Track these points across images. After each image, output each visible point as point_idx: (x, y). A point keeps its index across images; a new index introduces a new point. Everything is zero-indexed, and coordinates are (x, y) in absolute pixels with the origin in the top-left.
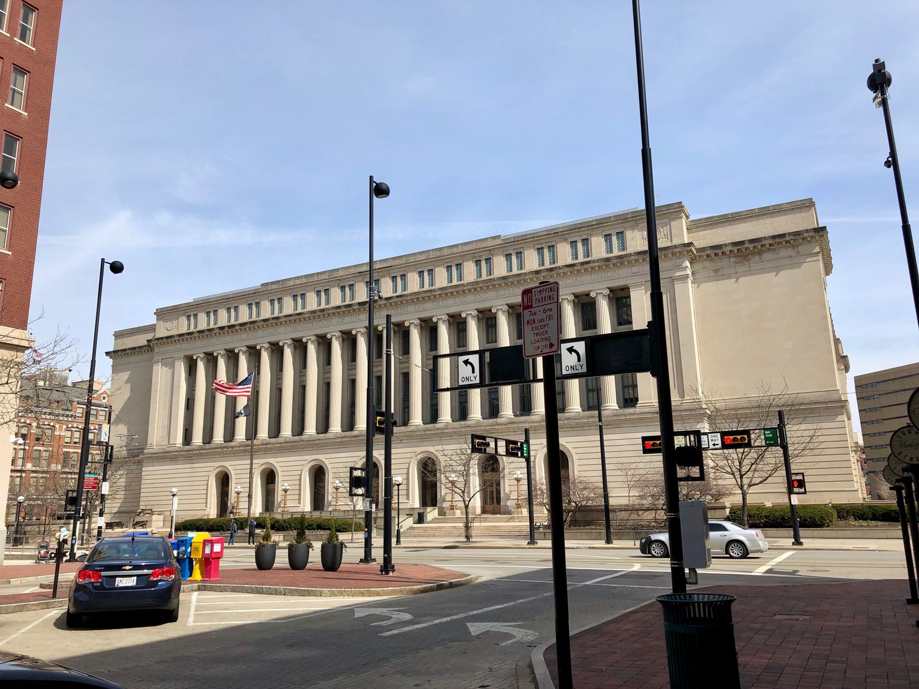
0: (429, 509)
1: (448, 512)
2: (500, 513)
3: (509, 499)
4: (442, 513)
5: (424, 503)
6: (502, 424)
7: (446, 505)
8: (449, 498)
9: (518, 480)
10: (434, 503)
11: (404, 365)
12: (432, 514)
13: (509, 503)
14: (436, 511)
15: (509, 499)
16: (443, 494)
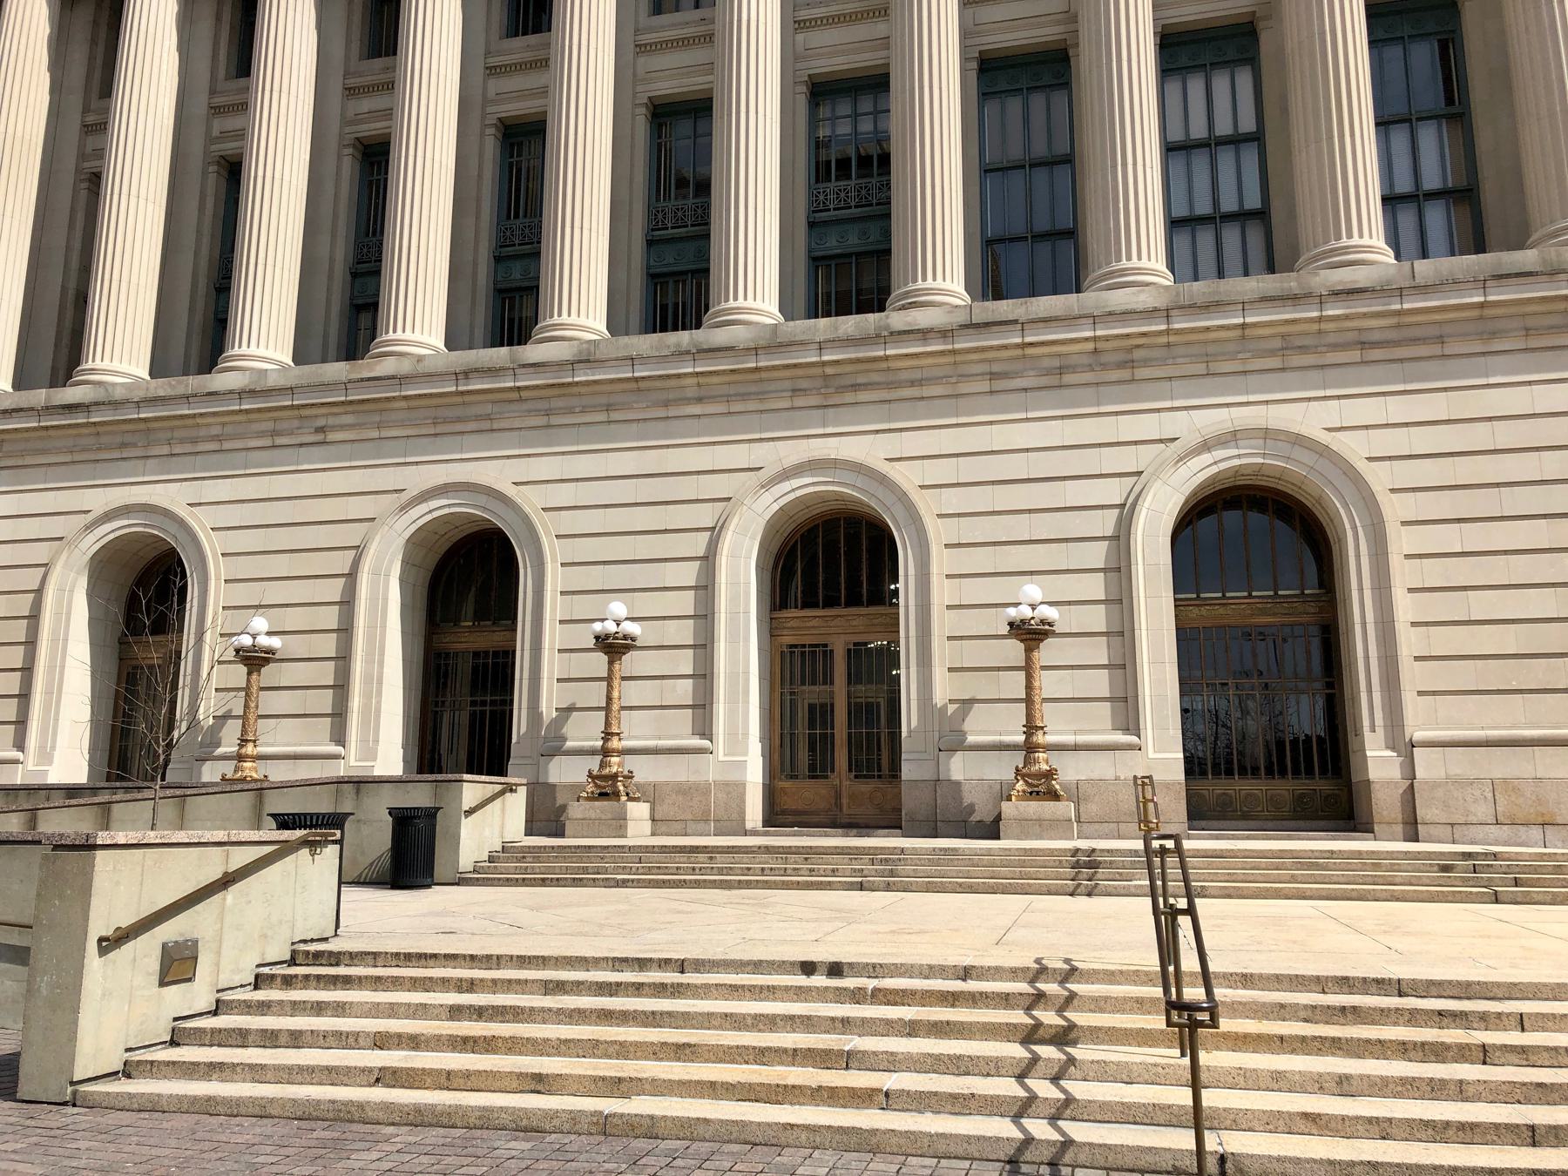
0: (472, 789)
1: (576, 810)
2: (892, 822)
3: (955, 743)
4: (546, 816)
5: (428, 754)
6: (924, 334)
7: (567, 772)
8: (584, 732)
9: (1030, 634)
10: (489, 752)
11: (366, 104)
12: (487, 819)
13: (959, 768)
14: (516, 806)
15: (955, 743)
16: (548, 710)
